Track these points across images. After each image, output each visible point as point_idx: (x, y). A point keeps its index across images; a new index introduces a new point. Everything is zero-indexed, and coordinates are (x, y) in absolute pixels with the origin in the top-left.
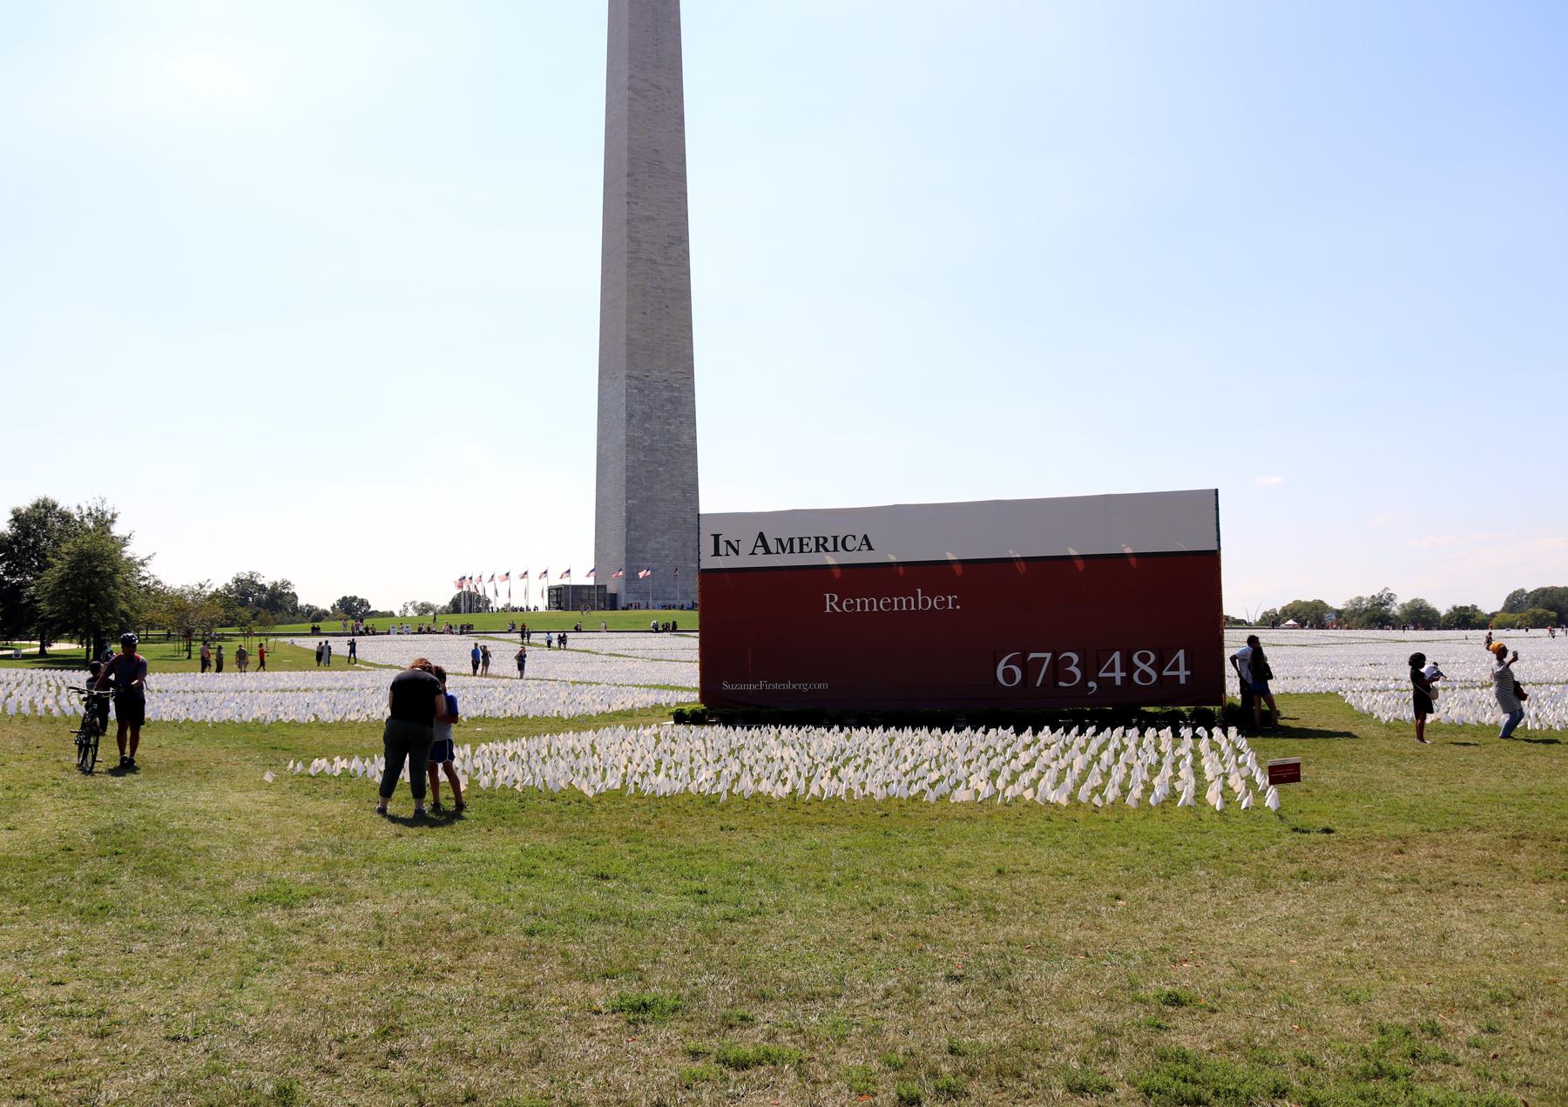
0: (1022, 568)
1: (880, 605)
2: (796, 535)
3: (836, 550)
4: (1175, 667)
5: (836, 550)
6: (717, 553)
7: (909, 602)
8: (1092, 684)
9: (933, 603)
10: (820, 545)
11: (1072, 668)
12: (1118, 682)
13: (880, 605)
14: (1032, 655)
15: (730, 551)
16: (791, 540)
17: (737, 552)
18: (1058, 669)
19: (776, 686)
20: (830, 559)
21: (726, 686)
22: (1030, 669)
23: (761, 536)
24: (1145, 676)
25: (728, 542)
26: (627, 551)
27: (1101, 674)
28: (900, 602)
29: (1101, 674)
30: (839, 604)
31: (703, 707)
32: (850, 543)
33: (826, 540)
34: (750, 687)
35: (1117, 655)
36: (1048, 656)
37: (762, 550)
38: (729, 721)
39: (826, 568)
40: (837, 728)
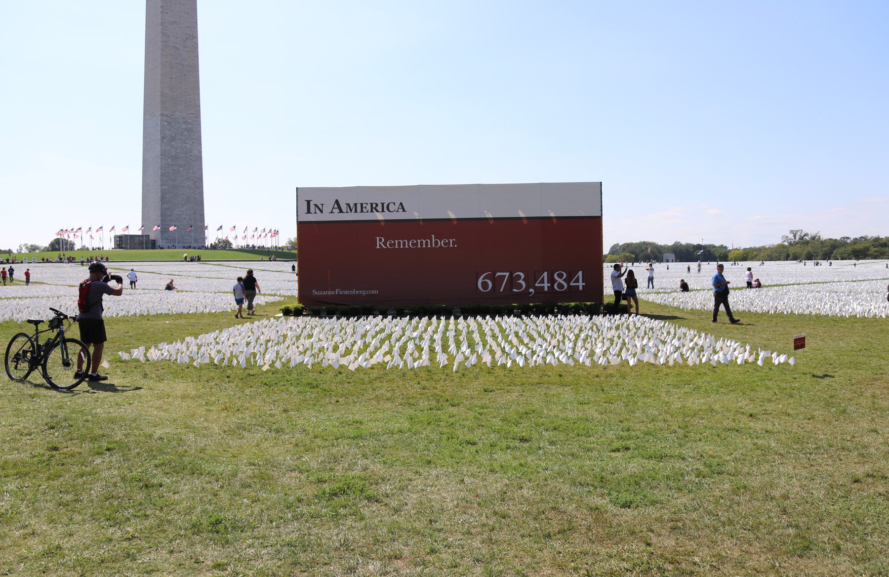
0: (525, 222)
1: (409, 244)
2: (359, 202)
3: (383, 211)
4: (577, 281)
5: (383, 211)
6: (309, 212)
7: (427, 243)
8: (531, 290)
9: (441, 243)
10: (374, 208)
11: (521, 281)
12: (546, 289)
13: (409, 244)
14: (498, 274)
15: (317, 211)
16: (356, 205)
17: (322, 212)
18: (512, 281)
19: (346, 292)
20: (379, 216)
21: (315, 292)
22: (497, 282)
23: (337, 202)
24: (560, 286)
25: (316, 205)
26: (162, 216)
27: (537, 285)
28: (422, 243)
29: (537, 285)
30: (385, 244)
31: (301, 305)
32: (392, 207)
33: (377, 205)
34: (330, 293)
35: (545, 274)
36: (507, 274)
37: (338, 210)
38: (316, 313)
39: (378, 221)
40: (335, 318)
